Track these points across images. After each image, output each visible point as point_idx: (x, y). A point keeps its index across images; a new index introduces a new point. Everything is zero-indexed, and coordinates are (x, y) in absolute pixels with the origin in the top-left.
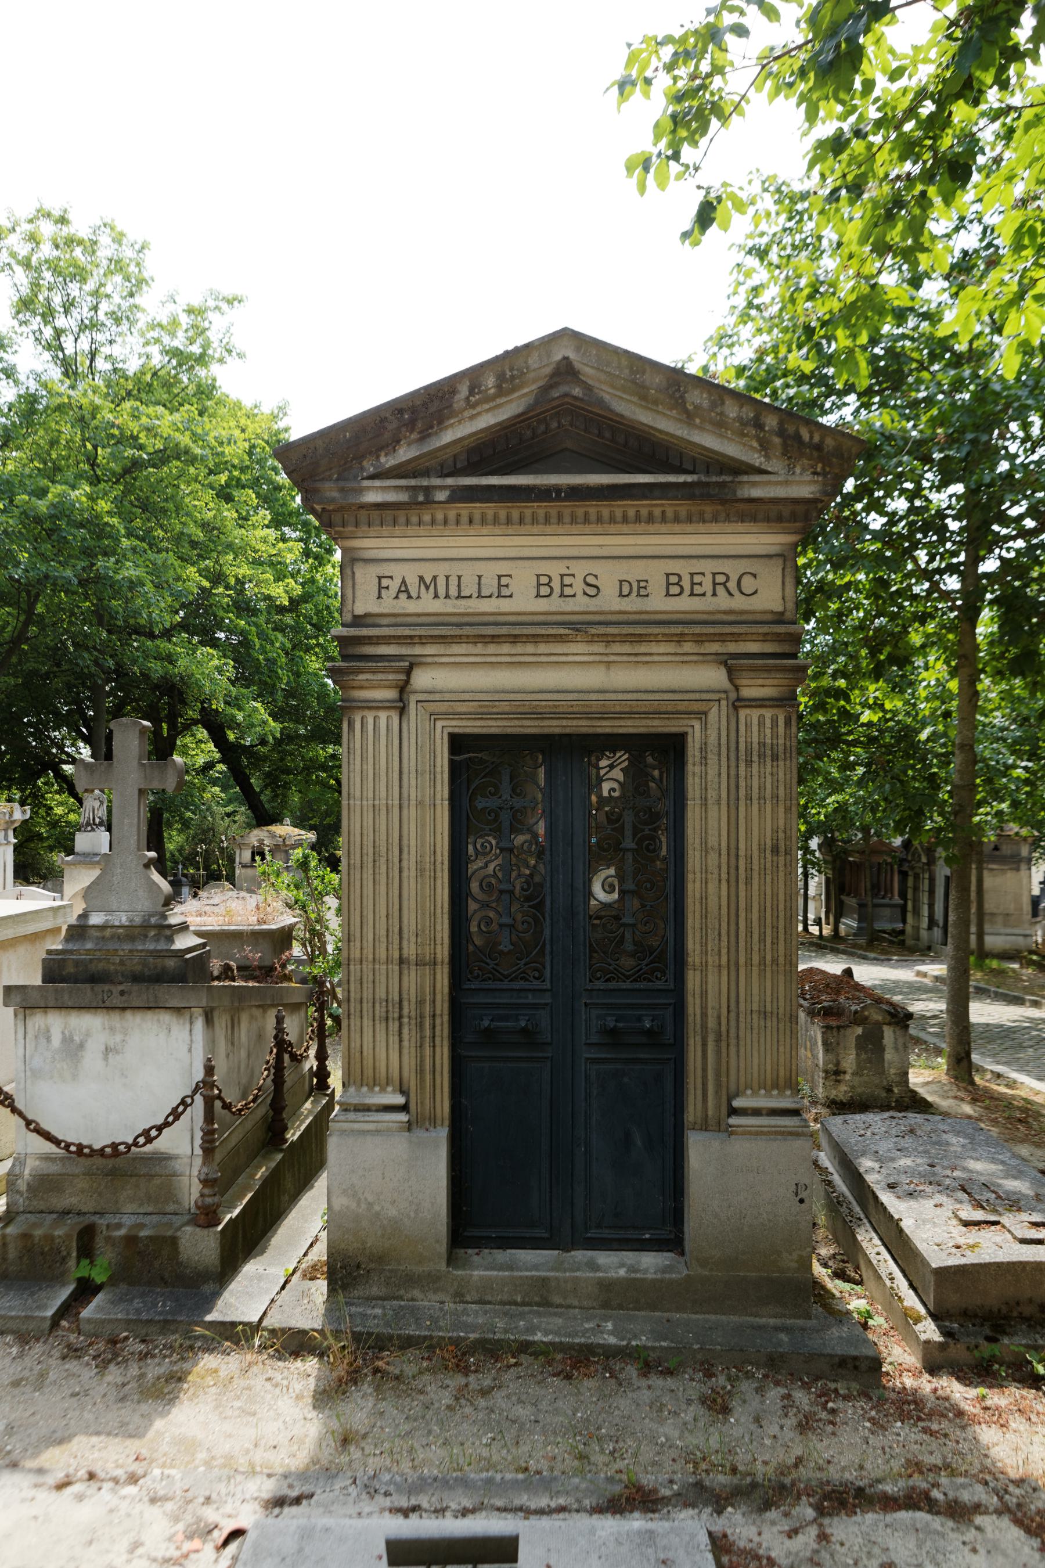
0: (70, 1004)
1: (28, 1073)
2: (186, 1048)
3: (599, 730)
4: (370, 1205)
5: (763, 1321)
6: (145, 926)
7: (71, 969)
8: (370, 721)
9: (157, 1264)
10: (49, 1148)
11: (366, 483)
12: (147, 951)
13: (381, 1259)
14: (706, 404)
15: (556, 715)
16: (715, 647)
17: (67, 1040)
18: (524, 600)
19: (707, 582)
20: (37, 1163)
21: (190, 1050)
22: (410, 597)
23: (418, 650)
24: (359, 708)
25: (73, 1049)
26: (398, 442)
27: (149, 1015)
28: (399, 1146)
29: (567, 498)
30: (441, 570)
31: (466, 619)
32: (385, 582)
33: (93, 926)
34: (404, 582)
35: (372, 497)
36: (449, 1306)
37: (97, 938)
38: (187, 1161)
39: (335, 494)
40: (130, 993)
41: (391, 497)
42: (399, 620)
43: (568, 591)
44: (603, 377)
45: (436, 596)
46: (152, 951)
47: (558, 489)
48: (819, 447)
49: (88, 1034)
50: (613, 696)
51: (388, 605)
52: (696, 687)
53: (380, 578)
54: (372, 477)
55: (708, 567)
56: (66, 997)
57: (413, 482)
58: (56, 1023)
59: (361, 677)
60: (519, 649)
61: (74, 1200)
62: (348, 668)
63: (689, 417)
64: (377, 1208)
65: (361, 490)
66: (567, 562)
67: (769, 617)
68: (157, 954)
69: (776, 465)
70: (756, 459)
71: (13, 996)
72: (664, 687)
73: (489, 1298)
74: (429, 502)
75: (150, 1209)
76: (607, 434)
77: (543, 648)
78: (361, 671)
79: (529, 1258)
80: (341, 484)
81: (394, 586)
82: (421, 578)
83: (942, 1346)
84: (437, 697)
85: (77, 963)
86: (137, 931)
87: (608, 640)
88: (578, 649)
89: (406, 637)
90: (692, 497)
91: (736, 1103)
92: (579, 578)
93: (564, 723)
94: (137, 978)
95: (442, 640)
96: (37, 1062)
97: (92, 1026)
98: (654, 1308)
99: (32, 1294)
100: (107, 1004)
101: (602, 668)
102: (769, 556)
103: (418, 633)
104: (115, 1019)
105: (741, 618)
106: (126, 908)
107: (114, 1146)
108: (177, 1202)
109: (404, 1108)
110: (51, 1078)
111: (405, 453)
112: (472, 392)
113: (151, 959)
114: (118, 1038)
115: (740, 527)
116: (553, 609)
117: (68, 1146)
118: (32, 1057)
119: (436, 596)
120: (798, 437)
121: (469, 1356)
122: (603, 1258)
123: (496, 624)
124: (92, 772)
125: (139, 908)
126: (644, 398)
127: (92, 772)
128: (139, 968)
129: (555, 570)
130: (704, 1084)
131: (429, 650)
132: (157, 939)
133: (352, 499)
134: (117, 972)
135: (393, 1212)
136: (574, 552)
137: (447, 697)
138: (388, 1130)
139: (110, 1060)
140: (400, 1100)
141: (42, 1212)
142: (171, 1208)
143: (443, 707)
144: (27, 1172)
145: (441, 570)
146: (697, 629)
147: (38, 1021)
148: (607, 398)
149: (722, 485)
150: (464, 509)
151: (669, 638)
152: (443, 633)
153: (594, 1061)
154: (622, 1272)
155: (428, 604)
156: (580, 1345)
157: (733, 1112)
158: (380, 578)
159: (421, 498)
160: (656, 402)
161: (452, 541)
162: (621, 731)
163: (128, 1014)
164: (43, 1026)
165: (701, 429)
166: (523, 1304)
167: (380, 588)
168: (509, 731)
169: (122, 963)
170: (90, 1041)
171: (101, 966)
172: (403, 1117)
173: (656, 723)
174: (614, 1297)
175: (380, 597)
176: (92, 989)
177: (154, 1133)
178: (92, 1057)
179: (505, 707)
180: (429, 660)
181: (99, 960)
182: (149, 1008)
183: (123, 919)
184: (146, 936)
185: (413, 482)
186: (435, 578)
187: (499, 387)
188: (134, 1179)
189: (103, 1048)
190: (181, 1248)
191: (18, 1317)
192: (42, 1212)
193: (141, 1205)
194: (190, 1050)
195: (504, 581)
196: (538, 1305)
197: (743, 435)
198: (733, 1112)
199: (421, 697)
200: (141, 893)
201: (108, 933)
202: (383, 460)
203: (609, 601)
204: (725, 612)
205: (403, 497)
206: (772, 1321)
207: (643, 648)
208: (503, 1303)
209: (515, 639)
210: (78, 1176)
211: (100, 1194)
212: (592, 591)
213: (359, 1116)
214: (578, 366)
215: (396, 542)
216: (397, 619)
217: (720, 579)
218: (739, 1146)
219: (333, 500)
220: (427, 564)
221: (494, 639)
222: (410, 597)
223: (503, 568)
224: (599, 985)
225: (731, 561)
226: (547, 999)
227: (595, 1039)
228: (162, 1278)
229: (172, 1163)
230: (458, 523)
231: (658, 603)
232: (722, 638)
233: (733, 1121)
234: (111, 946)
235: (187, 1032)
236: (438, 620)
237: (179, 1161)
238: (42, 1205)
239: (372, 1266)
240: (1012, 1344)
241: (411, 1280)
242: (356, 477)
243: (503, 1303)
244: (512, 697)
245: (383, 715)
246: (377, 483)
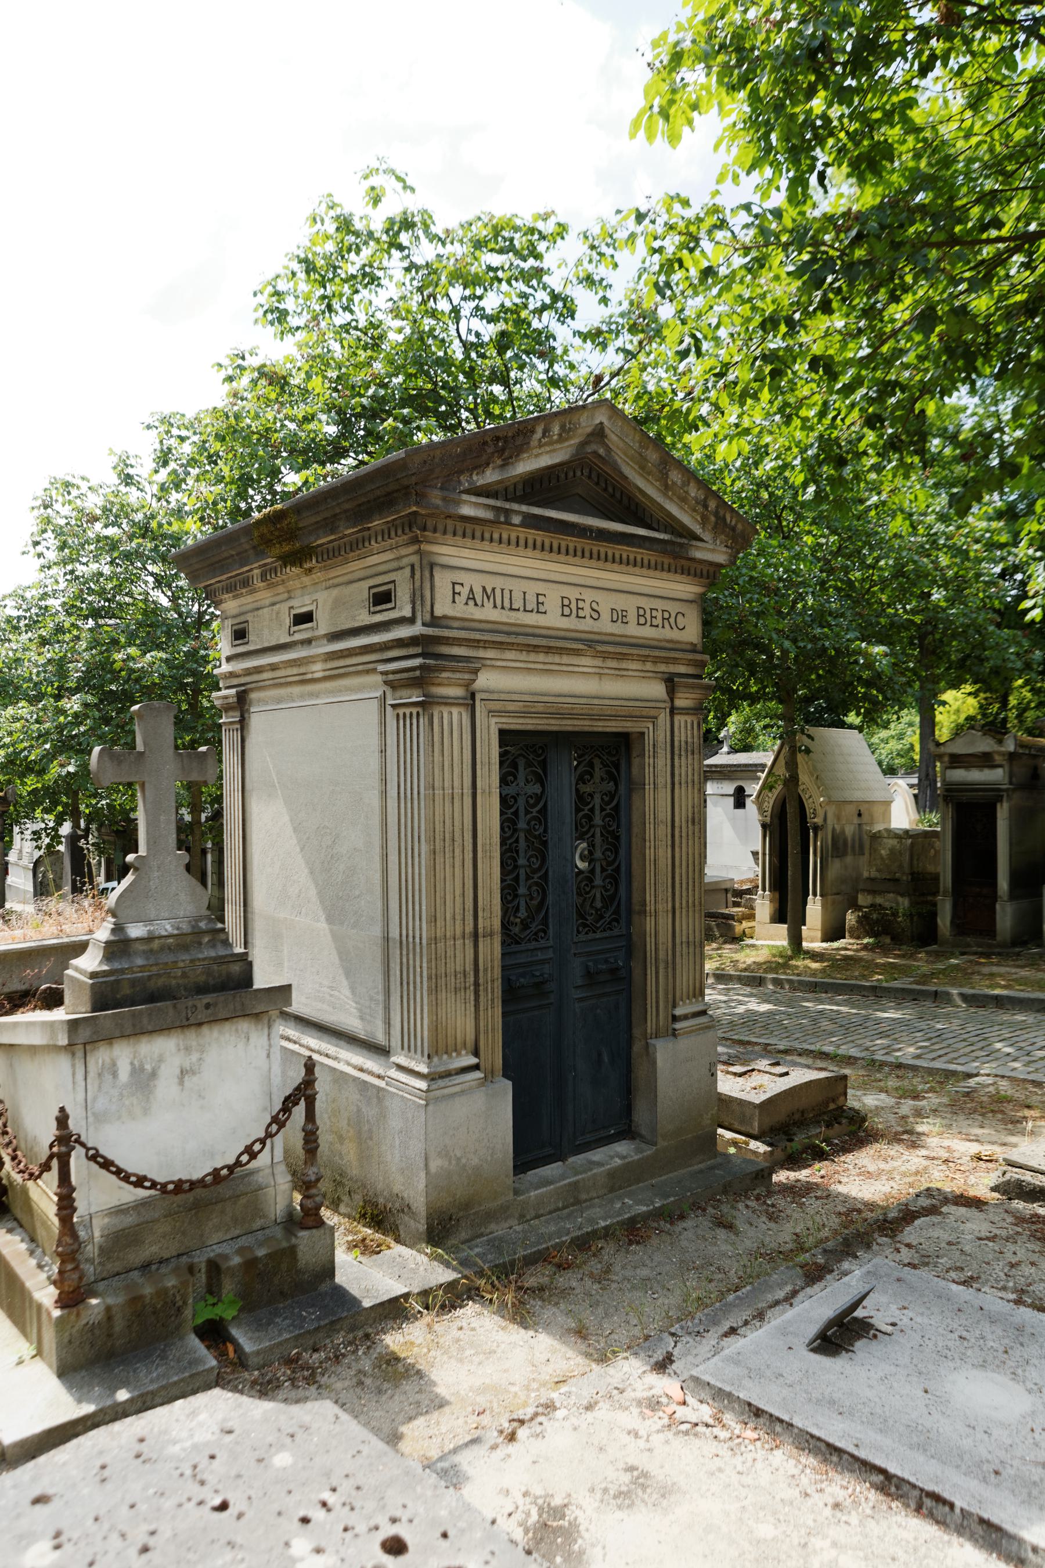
0: (150, 1028)
1: (91, 1119)
2: (264, 1055)
3: (596, 729)
4: (459, 1159)
5: (696, 1167)
6: (197, 933)
7: (126, 991)
8: (445, 715)
9: (276, 1281)
10: (131, 1194)
11: (465, 497)
12: (211, 958)
13: (467, 1206)
14: (679, 483)
15: (572, 716)
16: (662, 668)
17: (137, 1071)
18: (553, 619)
19: (659, 615)
20: (106, 1220)
21: (268, 1056)
22: (476, 604)
23: (481, 653)
24: (438, 703)
25: (144, 1080)
26: (488, 464)
27: (227, 1026)
28: (478, 1100)
29: (596, 539)
30: (498, 583)
31: (514, 629)
32: (458, 588)
33: (137, 939)
34: (471, 590)
35: (467, 511)
36: (518, 1228)
37: (144, 952)
38: (268, 1171)
39: (439, 502)
40: (216, 1004)
41: (481, 513)
42: (467, 624)
43: (581, 613)
44: (621, 445)
45: (495, 606)
46: (215, 959)
47: (550, 519)
48: (733, 529)
49: (161, 1059)
50: (607, 702)
51: (460, 610)
52: (649, 697)
53: (454, 584)
54: (468, 492)
55: (660, 604)
56: (145, 1021)
57: (499, 503)
58: (123, 1056)
59: (444, 675)
60: (550, 658)
61: (154, 1249)
62: (435, 666)
63: (666, 488)
64: (464, 1161)
65: (458, 503)
66: (580, 589)
67: (688, 647)
68: (220, 960)
69: (707, 536)
70: (697, 529)
71: (80, 1031)
72: (632, 696)
73: (541, 1212)
74: (508, 523)
75: (237, 1232)
76: (610, 490)
77: (565, 659)
78: (444, 669)
79: (549, 1172)
80: (446, 493)
81: (465, 592)
82: (484, 588)
83: (771, 1152)
84: (495, 696)
85: (133, 983)
86: (189, 939)
87: (605, 656)
88: (586, 662)
89: (474, 640)
90: (664, 552)
91: (678, 1012)
92: (588, 603)
93: (576, 722)
94: (201, 990)
95: (500, 646)
96: (101, 1104)
97: (164, 1051)
98: (638, 1181)
99: (163, 1357)
100: (192, 1021)
101: (597, 677)
102: (692, 602)
103: (485, 638)
104: (191, 1037)
105: (673, 646)
106: (166, 915)
107: (216, 1172)
108: (264, 1216)
109: (476, 1067)
110: (119, 1118)
111: (490, 476)
112: (544, 436)
113: (215, 967)
114: (195, 1057)
115: (678, 577)
116: (573, 627)
117: (164, 1185)
118: (95, 1099)
119: (495, 606)
120: (725, 519)
121: (560, 1258)
122: (597, 1155)
123: (534, 635)
124: (120, 763)
125: (182, 914)
126: (643, 468)
127: (120, 763)
128: (203, 978)
129: (573, 593)
130: (657, 1002)
131: (490, 654)
132: (212, 944)
133: (452, 510)
134: (179, 985)
135: (475, 1161)
136: (581, 581)
137: (503, 696)
138: (471, 1088)
139: (187, 1084)
140: (474, 1061)
141: (118, 1274)
142: (258, 1223)
143: (497, 706)
144: (97, 1234)
145: (498, 583)
146: (657, 653)
147: (101, 1056)
148: (619, 461)
149: (681, 545)
150: (532, 534)
151: (644, 659)
152: (499, 639)
153: (581, 1000)
154: (618, 1161)
155: (489, 613)
156: (629, 1219)
157: (675, 1019)
158: (454, 584)
159: (502, 519)
160: (649, 473)
161: (499, 558)
162: (608, 730)
163: (205, 1029)
164: (108, 1060)
165: (671, 499)
166: (564, 1208)
167: (454, 593)
168: (540, 728)
169: (184, 975)
170: (163, 1067)
171: (161, 982)
172: (478, 1075)
173: (629, 724)
174: (620, 1180)
175: (454, 602)
176: (175, 1006)
177: (257, 1147)
178: (166, 1086)
179: (540, 707)
180: (488, 662)
181: (159, 976)
182: (227, 1019)
183: (167, 928)
184: (200, 943)
185: (499, 503)
186: (494, 589)
187: (560, 435)
188: (220, 1206)
189: (178, 1071)
190: (300, 1254)
191: (182, 1380)
192: (118, 1274)
193: (227, 1231)
194: (268, 1056)
195: (541, 599)
196: (573, 1205)
197: (694, 510)
198: (675, 1019)
199: (484, 696)
200: (183, 897)
201: (156, 944)
202: (475, 478)
203: (606, 626)
204: (668, 641)
205: (489, 515)
206: (701, 1166)
207: (624, 665)
208: (550, 1213)
209: (548, 650)
210: (158, 1220)
211: (184, 1233)
212: (595, 616)
213: (446, 1082)
214: (607, 431)
215: (466, 553)
216: (466, 624)
217: (666, 615)
218: (683, 1043)
219: (437, 507)
220: (532, 582)
221: (535, 649)
222: (476, 604)
223: (540, 587)
224: (582, 937)
225: (670, 602)
226: (550, 954)
227: (579, 982)
228: (281, 1293)
229: (255, 1177)
230: (509, 544)
231: (633, 630)
232: (667, 661)
233: (678, 1026)
234: (170, 958)
235: (266, 1037)
236: (495, 628)
237: (261, 1174)
238: (117, 1266)
239: (461, 1214)
240: (800, 1139)
241: (491, 1216)
242: (455, 489)
243: (550, 1213)
244: (545, 699)
245: (455, 711)
246: (473, 499)
